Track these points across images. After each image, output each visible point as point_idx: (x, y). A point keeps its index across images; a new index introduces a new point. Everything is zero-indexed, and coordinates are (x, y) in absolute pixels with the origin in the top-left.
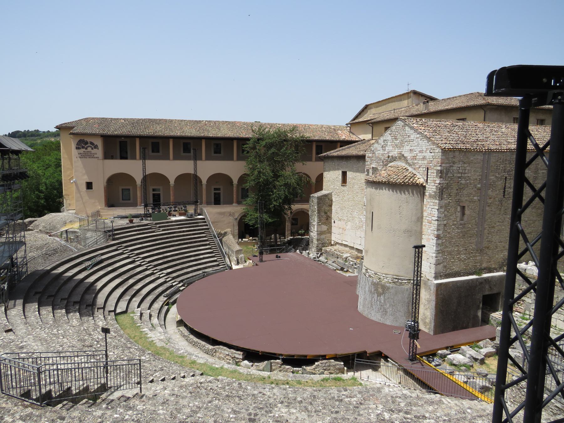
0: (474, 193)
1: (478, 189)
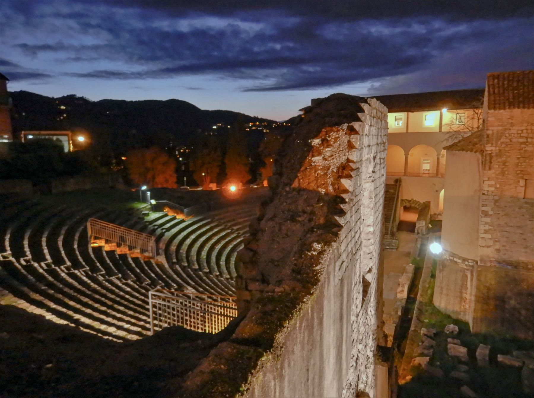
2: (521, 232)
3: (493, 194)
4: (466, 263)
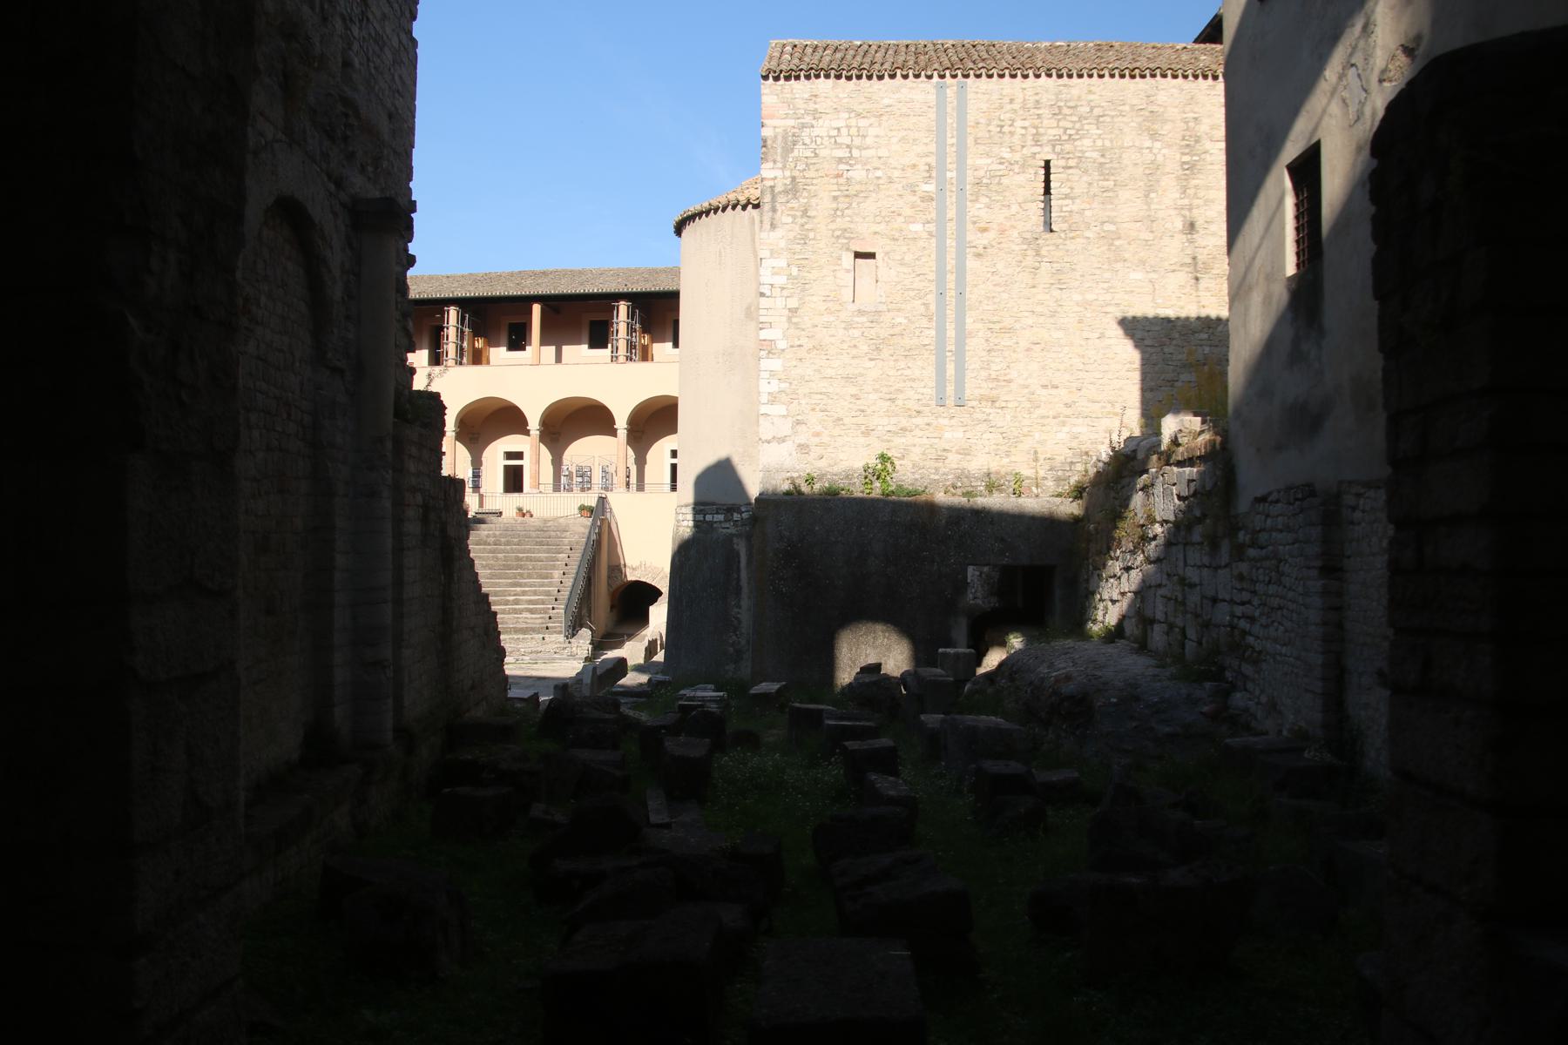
0: (908, 212)
1: (923, 199)
2: (853, 390)
3: (785, 293)
4: (736, 516)
